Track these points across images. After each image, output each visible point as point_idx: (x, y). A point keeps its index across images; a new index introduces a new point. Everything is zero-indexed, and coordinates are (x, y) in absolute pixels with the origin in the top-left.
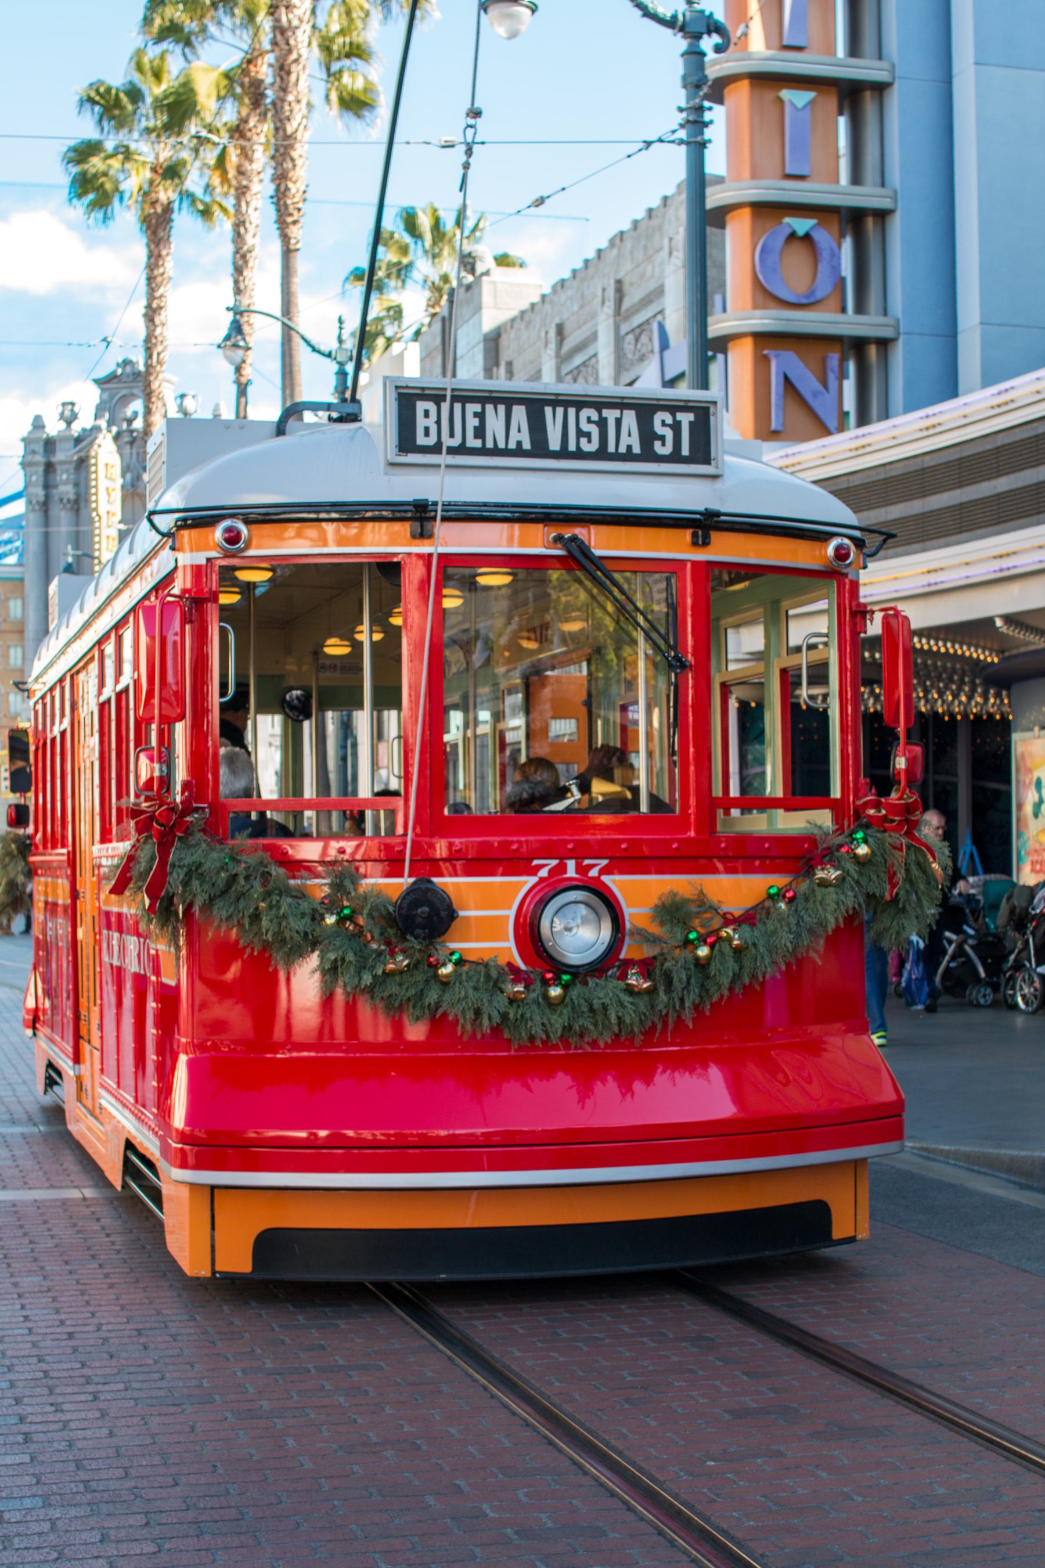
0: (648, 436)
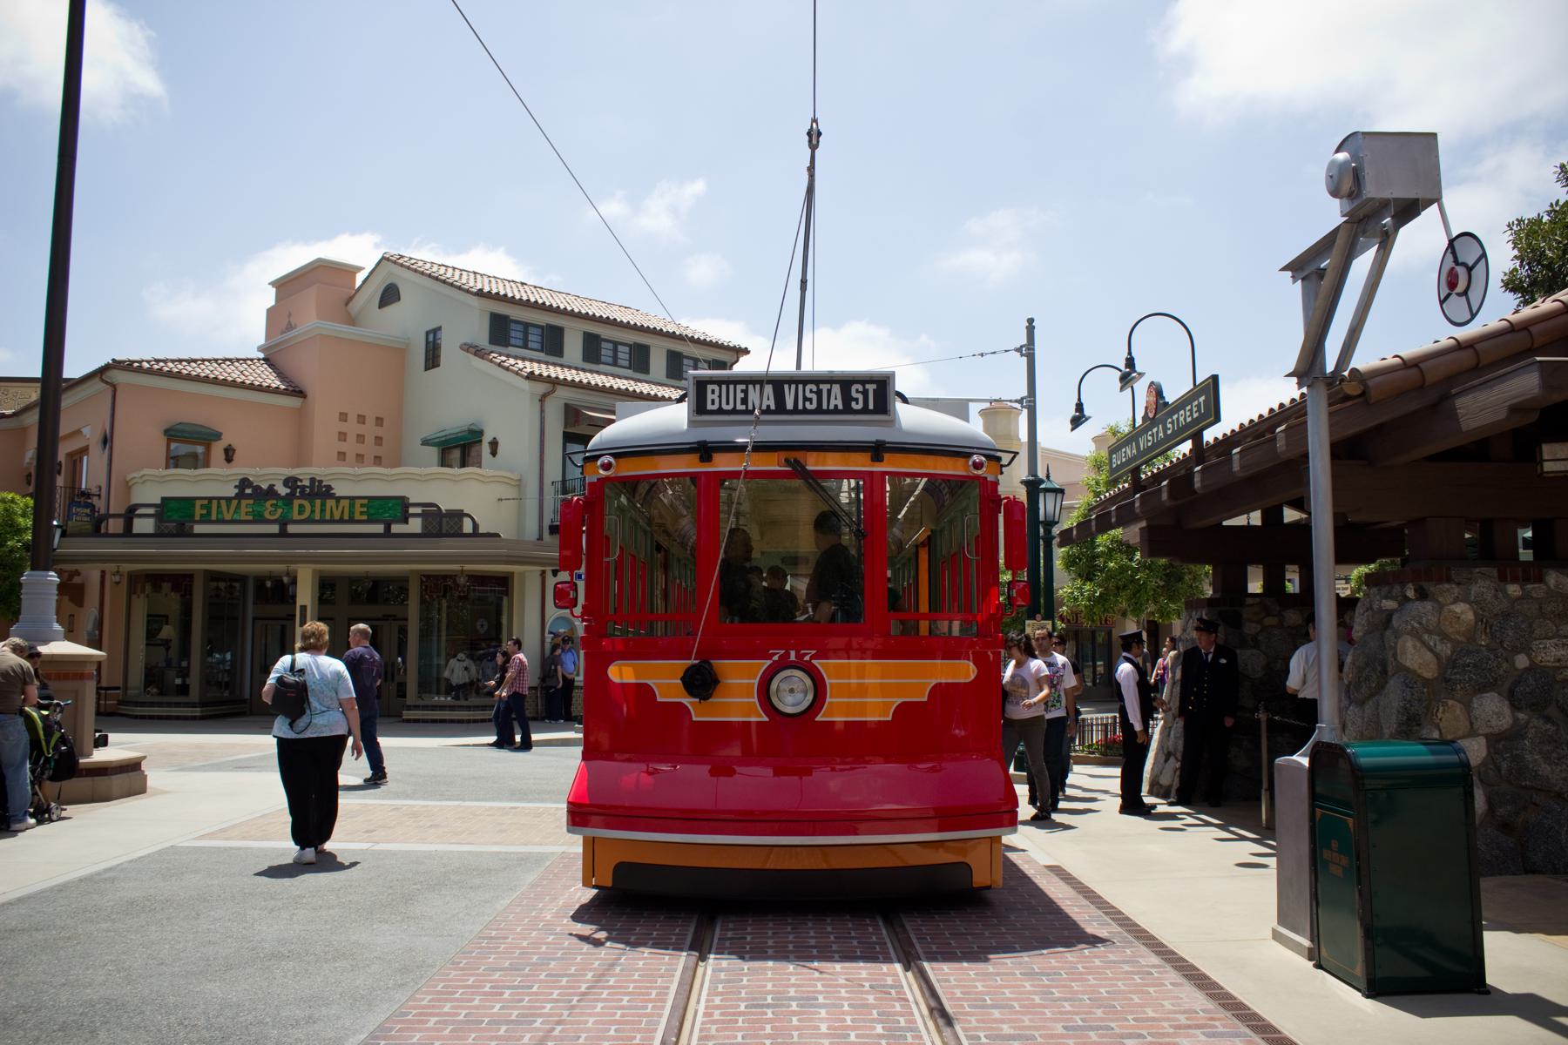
0: (847, 398)
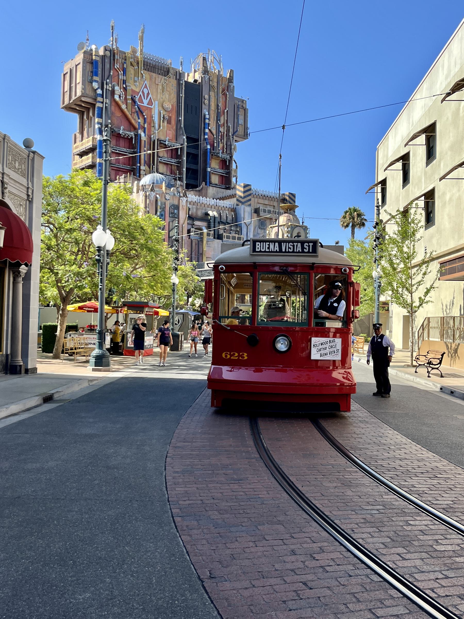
0: (303, 248)
